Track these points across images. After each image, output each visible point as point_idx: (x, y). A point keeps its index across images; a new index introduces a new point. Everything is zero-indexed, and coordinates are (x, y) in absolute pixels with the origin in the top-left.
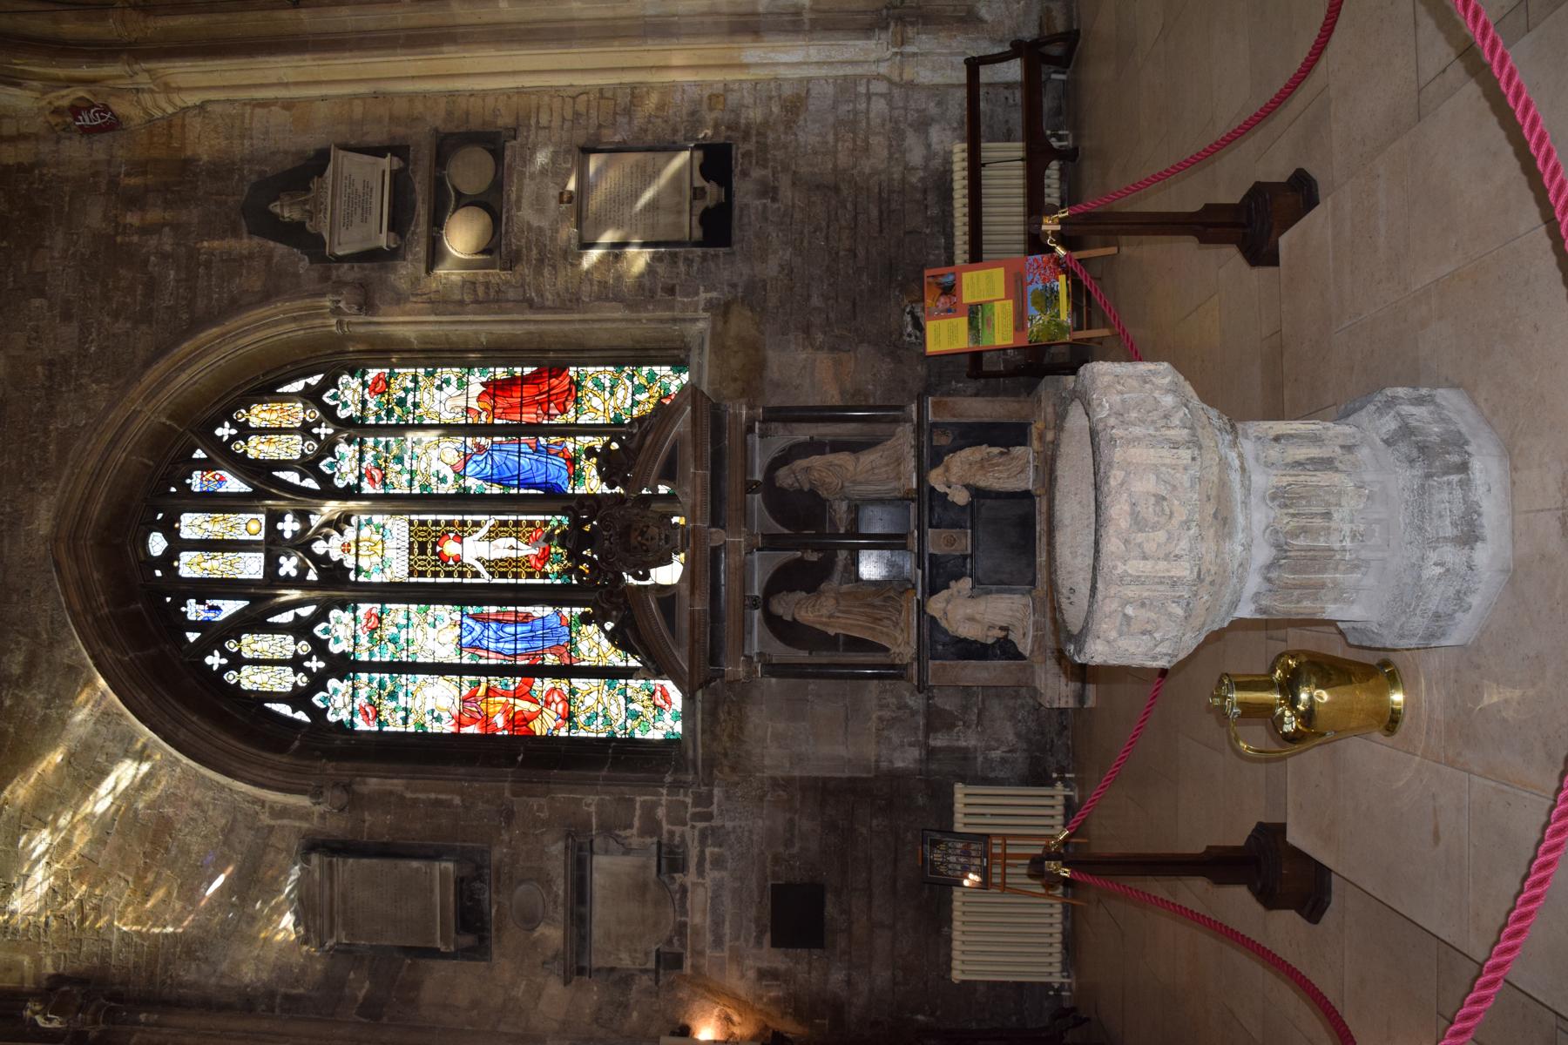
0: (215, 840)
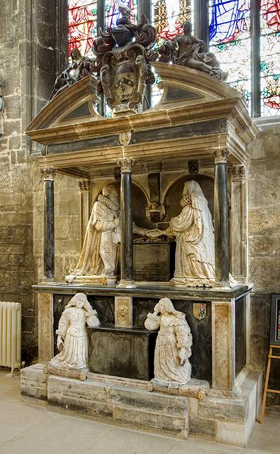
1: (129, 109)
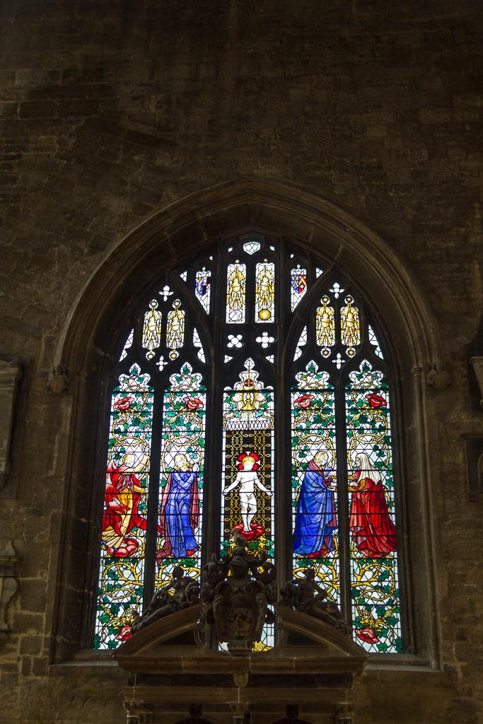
0: (33, 300)
1: (246, 648)
